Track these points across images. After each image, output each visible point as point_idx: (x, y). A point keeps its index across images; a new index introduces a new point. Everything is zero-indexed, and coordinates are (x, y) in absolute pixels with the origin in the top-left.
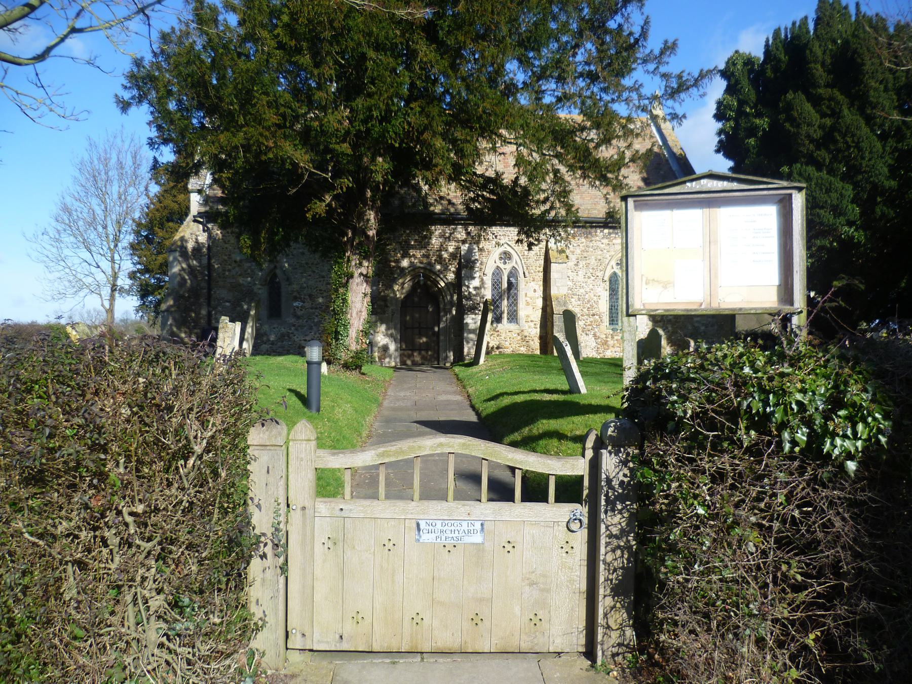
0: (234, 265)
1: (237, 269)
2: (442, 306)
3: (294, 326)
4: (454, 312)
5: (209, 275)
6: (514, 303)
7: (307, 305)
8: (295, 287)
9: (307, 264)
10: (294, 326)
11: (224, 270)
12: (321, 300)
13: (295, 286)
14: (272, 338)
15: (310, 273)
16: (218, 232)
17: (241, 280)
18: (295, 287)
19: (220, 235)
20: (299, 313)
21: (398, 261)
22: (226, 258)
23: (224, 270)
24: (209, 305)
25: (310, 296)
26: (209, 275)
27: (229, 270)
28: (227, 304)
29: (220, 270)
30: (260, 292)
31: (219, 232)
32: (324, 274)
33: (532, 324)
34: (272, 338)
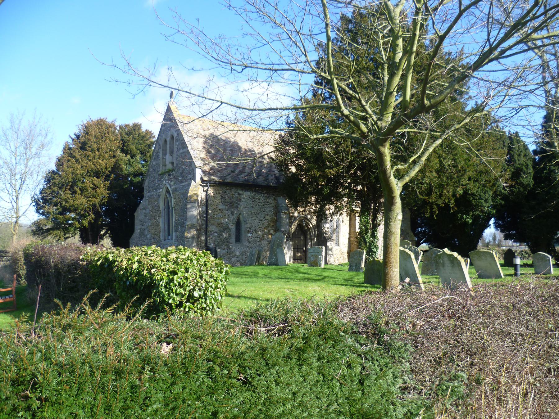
0: (219, 211)
1: (220, 214)
2: (309, 237)
3: (248, 247)
4: (315, 240)
5: (206, 217)
6: (338, 236)
7: (254, 235)
8: (249, 225)
9: (254, 213)
10: (248, 247)
11: (214, 215)
12: (260, 233)
13: (248, 225)
14: (238, 253)
15: (255, 218)
16: (211, 192)
17: (222, 221)
18: (249, 225)
19: (212, 194)
20: (250, 240)
21: (293, 213)
22: (215, 207)
23: (214, 215)
24: (206, 234)
25: (255, 230)
26: (206, 217)
27: (217, 215)
28: (215, 234)
29: (212, 214)
30: (232, 227)
31: (211, 192)
32: (262, 218)
33: (345, 246)
34: (238, 253)
